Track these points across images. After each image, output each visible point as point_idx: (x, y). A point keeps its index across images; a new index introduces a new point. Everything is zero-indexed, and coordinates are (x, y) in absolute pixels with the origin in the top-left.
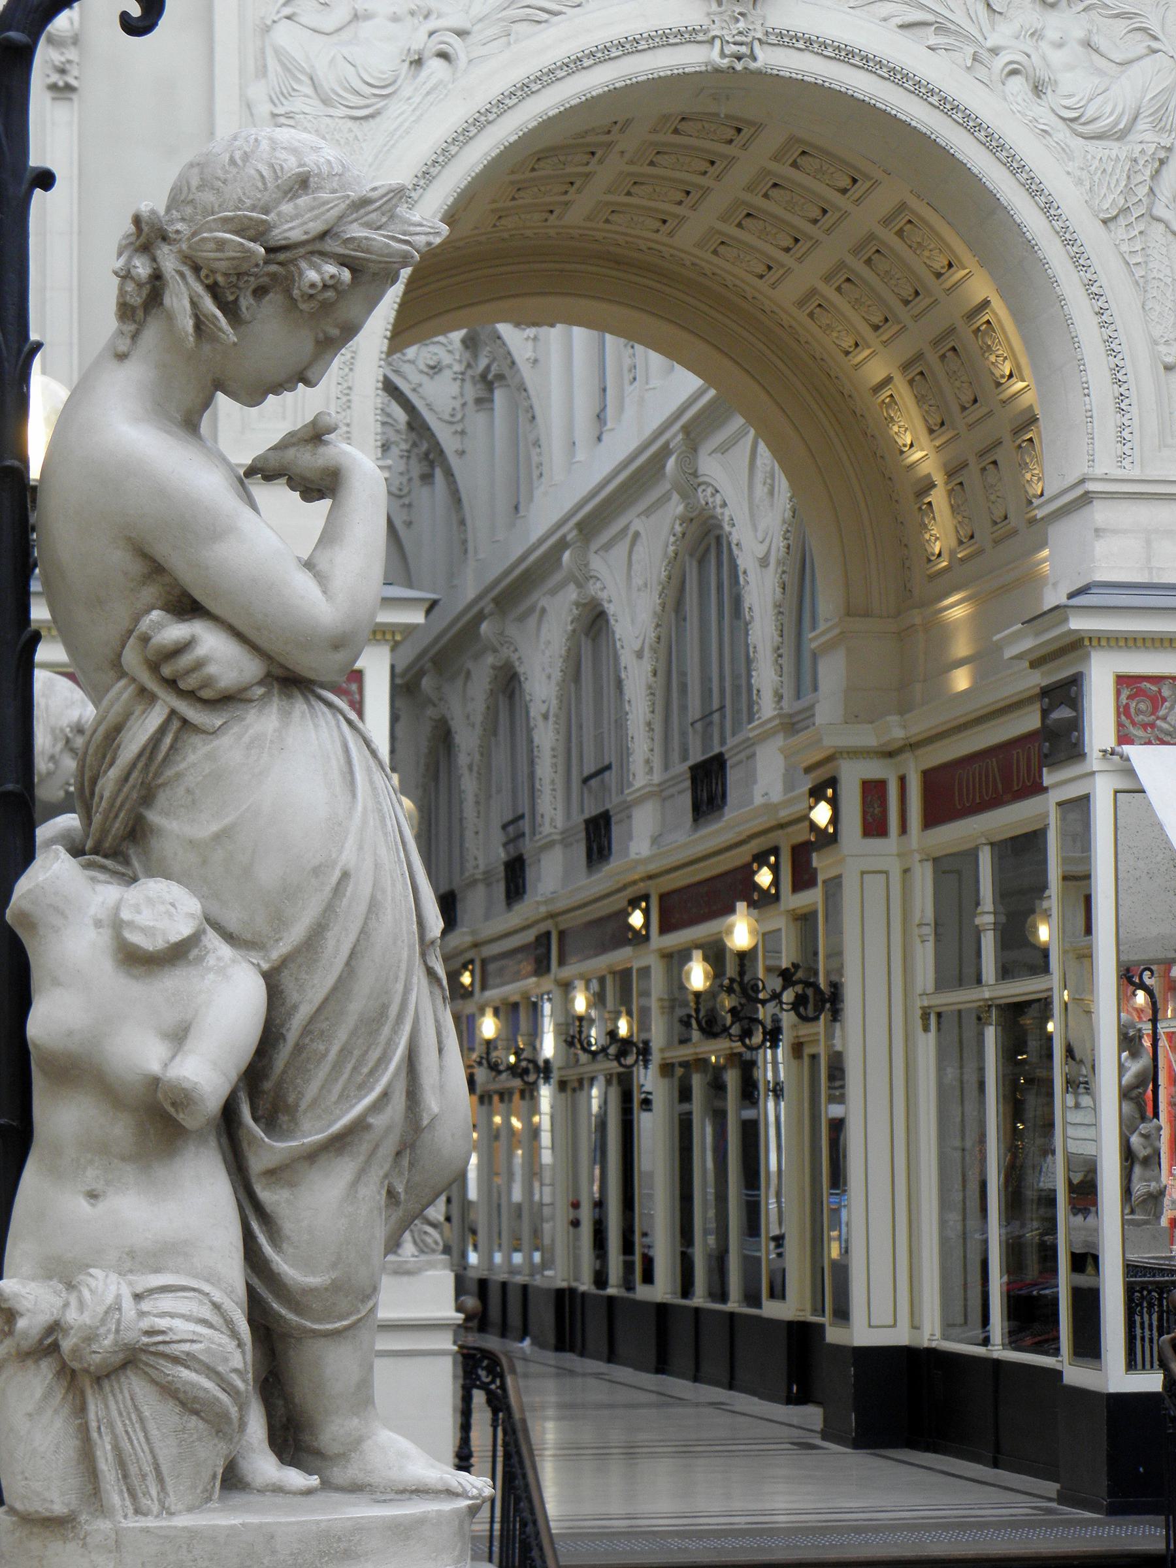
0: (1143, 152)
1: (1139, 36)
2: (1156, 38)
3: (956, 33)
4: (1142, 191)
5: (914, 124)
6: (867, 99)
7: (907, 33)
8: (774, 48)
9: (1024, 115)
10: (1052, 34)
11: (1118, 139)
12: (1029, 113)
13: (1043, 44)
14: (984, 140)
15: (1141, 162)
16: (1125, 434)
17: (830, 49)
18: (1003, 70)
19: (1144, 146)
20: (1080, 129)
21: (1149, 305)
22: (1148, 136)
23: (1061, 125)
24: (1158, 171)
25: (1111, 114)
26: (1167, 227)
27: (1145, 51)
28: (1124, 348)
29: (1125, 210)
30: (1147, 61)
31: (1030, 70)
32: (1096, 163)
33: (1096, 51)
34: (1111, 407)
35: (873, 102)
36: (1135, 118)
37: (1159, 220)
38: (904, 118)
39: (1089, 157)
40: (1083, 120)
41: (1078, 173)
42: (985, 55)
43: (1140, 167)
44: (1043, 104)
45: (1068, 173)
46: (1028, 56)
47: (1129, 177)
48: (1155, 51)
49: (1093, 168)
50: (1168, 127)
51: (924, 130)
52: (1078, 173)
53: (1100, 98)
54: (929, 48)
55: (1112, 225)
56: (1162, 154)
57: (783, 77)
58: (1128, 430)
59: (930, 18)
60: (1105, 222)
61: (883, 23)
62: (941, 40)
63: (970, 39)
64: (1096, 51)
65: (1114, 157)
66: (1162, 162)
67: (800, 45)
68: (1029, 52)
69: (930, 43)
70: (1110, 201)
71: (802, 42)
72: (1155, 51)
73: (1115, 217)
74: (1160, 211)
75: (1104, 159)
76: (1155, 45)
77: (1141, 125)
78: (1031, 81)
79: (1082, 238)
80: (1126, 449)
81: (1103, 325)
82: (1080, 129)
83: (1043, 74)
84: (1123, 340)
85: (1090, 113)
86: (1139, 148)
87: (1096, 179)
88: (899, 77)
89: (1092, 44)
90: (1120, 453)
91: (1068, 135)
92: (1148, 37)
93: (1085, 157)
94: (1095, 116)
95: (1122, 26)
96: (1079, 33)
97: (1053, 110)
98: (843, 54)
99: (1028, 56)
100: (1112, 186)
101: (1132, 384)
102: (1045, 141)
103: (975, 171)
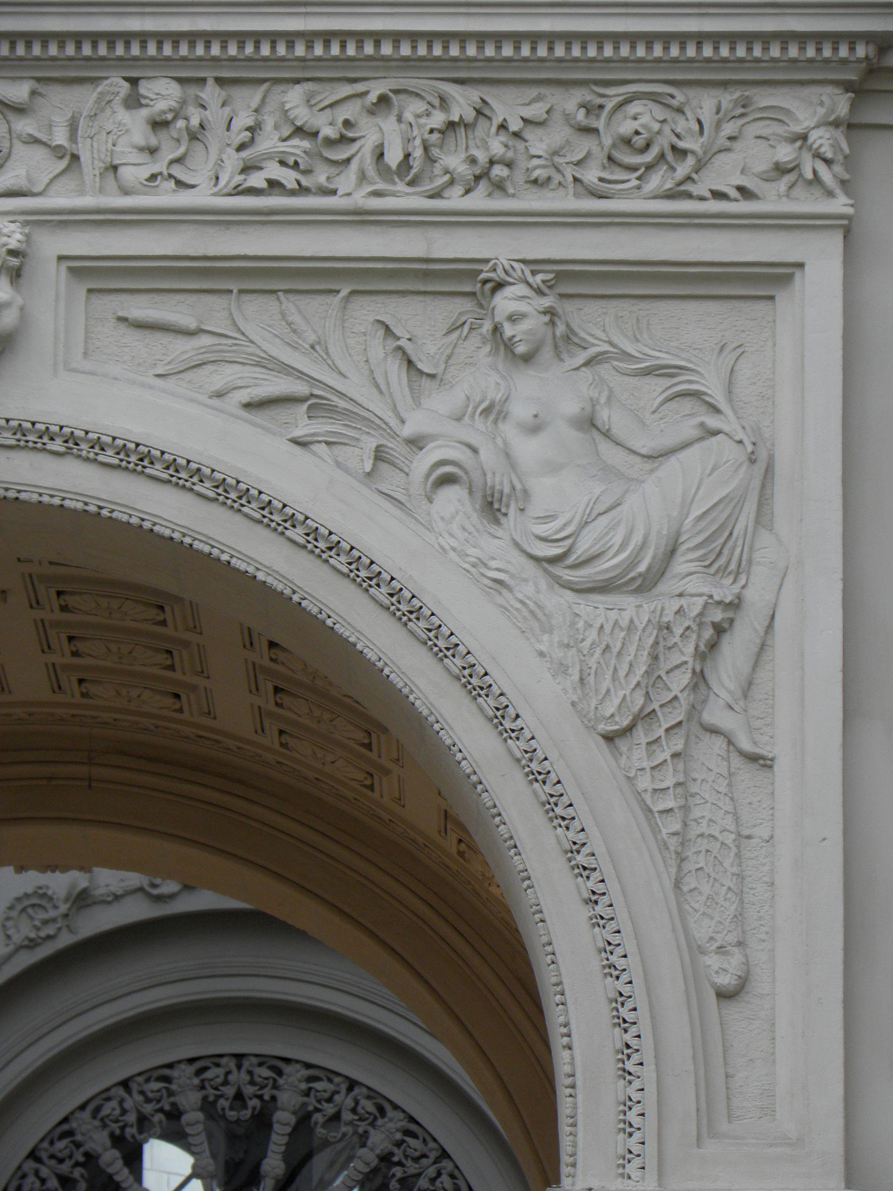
0: (679, 611)
1: (687, 405)
2: (715, 410)
3: (346, 413)
4: (680, 681)
5: (261, 576)
6: (176, 535)
7: (257, 417)
8: (12, 454)
9: (463, 555)
10: (521, 411)
11: (639, 591)
12: (471, 551)
13: (508, 429)
14: (386, 601)
15: (678, 631)
16: (632, 1117)
17: (110, 452)
18: (428, 476)
19: (683, 601)
20: (568, 575)
21: (690, 882)
22: (693, 585)
23: (531, 570)
24: (713, 646)
25: (623, 547)
26: (730, 742)
27: (695, 433)
28: (633, 962)
29: (646, 716)
30: (695, 449)
31: (476, 476)
32: (593, 635)
33: (607, 435)
34: (611, 1068)
35: (187, 540)
36: (672, 553)
37: (714, 731)
38: (243, 567)
39: (581, 625)
40: (571, 560)
41: (558, 654)
42: (397, 449)
43: (677, 639)
44: (500, 533)
45: (541, 654)
46: (475, 450)
47: (655, 658)
48: (715, 433)
49: (587, 644)
50: (733, 566)
51: (280, 587)
52: (558, 654)
53: (604, 521)
54: (296, 442)
55: (623, 745)
56: (718, 615)
57: (25, 502)
58: (637, 1109)
59: (300, 388)
60: (609, 738)
61: (215, 402)
62: (321, 427)
63: (371, 423)
64: (607, 435)
65: (624, 623)
66: (720, 630)
67: (57, 446)
68: (473, 441)
69: (298, 433)
70: (616, 701)
71: (59, 441)
72: (715, 433)
73: (629, 729)
74: (714, 715)
75: (608, 628)
76: (713, 422)
77: (682, 564)
78: (479, 495)
79: (559, 769)
80: (633, 1143)
81: (599, 921)
82: (568, 575)
83: (500, 480)
84: (630, 947)
85: (584, 547)
86: (675, 604)
87: (592, 662)
88: (233, 495)
89: (599, 424)
90: (621, 1151)
91: (543, 584)
92: (704, 408)
93: (573, 624)
94: (594, 550)
95: (656, 388)
96: (571, 407)
97: (517, 545)
98: (133, 459)
99: (475, 450)
100: (622, 674)
101: (645, 1026)
102: (500, 600)
103: (371, 655)
